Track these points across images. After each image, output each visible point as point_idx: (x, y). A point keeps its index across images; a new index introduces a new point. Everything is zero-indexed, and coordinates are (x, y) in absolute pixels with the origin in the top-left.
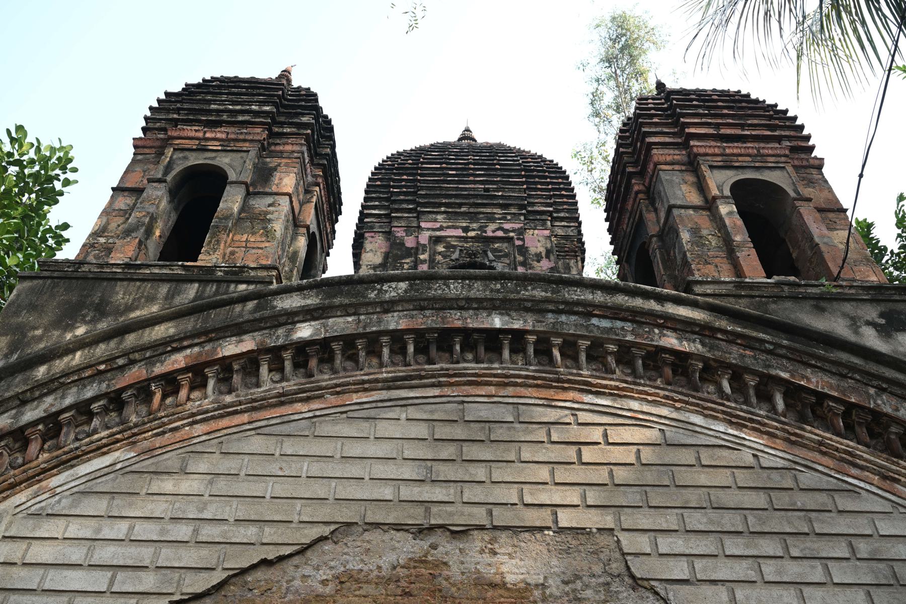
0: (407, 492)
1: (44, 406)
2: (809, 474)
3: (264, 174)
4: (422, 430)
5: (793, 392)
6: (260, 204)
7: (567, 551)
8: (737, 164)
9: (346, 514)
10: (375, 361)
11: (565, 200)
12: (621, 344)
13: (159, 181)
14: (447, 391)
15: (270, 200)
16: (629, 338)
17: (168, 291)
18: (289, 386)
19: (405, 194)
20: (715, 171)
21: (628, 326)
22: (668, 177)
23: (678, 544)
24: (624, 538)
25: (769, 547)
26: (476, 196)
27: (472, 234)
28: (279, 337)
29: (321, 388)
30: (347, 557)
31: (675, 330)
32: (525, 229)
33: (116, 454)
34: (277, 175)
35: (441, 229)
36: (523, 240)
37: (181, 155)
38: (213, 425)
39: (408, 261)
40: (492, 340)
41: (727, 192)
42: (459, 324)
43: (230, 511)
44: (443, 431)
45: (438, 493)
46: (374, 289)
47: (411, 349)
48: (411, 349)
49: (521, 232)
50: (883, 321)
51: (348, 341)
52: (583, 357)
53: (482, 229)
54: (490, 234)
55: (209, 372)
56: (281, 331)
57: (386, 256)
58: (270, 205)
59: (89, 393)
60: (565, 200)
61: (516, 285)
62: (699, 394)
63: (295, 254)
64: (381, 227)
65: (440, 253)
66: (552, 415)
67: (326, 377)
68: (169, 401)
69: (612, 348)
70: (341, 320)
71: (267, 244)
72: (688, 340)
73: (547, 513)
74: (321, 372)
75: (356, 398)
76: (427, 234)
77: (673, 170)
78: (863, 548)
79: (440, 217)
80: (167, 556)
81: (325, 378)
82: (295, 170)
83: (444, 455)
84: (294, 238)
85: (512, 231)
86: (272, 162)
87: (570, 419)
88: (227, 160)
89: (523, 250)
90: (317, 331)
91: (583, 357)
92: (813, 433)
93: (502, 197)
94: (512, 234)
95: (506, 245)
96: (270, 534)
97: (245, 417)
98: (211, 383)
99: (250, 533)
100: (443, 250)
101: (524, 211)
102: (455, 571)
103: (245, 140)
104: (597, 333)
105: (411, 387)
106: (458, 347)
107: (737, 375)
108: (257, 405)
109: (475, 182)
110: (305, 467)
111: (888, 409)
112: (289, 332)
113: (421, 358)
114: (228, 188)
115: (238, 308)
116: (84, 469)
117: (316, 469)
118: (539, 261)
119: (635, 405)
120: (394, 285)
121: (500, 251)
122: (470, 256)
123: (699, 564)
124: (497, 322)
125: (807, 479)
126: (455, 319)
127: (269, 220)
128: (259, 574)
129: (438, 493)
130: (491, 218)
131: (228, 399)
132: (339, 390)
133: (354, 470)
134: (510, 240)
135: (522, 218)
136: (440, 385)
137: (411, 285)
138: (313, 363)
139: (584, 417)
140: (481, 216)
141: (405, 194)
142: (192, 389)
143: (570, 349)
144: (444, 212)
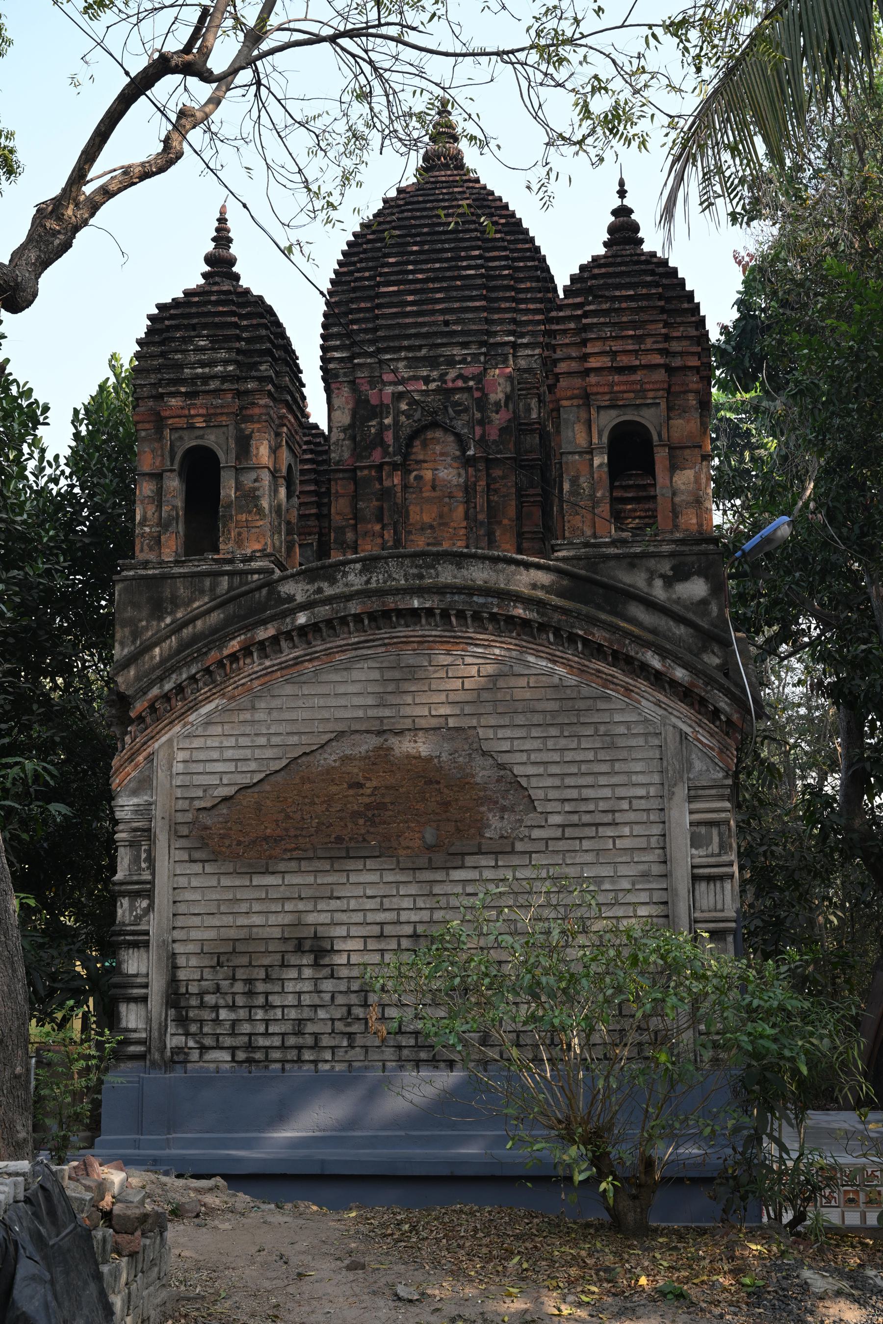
0: (371, 713)
1: (173, 680)
2: (587, 688)
3: (244, 445)
4: (376, 675)
5: (586, 642)
6: (248, 479)
7: (452, 739)
8: (621, 403)
9: (340, 727)
10: (346, 629)
11: (531, 317)
13: (171, 471)
15: (253, 475)
16: (495, 610)
18: (298, 653)
19: (366, 331)
20: (602, 412)
21: (495, 601)
22: (565, 416)
23: (508, 733)
24: (480, 731)
25: (554, 731)
26: (435, 334)
27: (433, 386)
29: (316, 652)
30: (345, 748)
31: (523, 603)
32: (485, 369)
33: (217, 701)
34: (253, 442)
37: (177, 435)
38: (263, 680)
39: (374, 423)
40: (415, 613)
41: (605, 439)
42: (392, 606)
43: (281, 729)
44: (388, 675)
45: (387, 712)
46: (340, 571)
47: (366, 622)
48: (366, 622)
49: (479, 378)
50: (671, 573)
51: (329, 622)
52: (469, 621)
53: (442, 378)
54: (450, 385)
56: (288, 620)
57: (354, 414)
58: (256, 481)
59: (194, 671)
60: (531, 317)
61: (433, 560)
62: (538, 641)
63: (279, 506)
64: (345, 375)
65: (403, 412)
66: (448, 660)
67: (319, 643)
68: (234, 666)
69: (485, 615)
70: (322, 609)
71: (261, 523)
72: (530, 610)
73: (442, 720)
74: (315, 639)
75: (338, 657)
76: (389, 390)
77: (572, 406)
78: (602, 729)
79: (401, 365)
80: (258, 753)
81: (319, 646)
82: (266, 435)
83: (389, 690)
84: (276, 491)
85: (472, 379)
86: (248, 427)
87: (459, 662)
88: (213, 438)
89: (482, 404)
90: (309, 619)
91: (469, 621)
93: (462, 333)
94: (471, 383)
95: (466, 395)
96: (304, 739)
97: (279, 674)
98: (255, 655)
99: (295, 739)
100: (406, 407)
101: (484, 350)
102: (397, 752)
103: (222, 414)
104: (476, 608)
105: (369, 647)
106: (394, 619)
107: (557, 632)
109: (433, 312)
111: (632, 653)
112: (294, 620)
113: (373, 625)
114: (222, 473)
116: (204, 710)
117: (322, 702)
118: (497, 413)
119: (497, 651)
120: (352, 566)
121: (460, 404)
122: (431, 414)
123: (516, 743)
124: (416, 604)
125: (585, 691)
126: (391, 602)
127: (258, 497)
128: (304, 759)
129: (387, 712)
130: (451, 362)
131: (268, 663)
132: (328, 653)
133: (342, 702)
134: (469, 389)
135: (482, 358)
136: (385, 645)
137: (363, 566)
138: (310, 636)
139: (469, 660)
140: (442, 359)
141: (366, 331)
142: (245, 656)
143: (461, 615)
144: (406, 358)
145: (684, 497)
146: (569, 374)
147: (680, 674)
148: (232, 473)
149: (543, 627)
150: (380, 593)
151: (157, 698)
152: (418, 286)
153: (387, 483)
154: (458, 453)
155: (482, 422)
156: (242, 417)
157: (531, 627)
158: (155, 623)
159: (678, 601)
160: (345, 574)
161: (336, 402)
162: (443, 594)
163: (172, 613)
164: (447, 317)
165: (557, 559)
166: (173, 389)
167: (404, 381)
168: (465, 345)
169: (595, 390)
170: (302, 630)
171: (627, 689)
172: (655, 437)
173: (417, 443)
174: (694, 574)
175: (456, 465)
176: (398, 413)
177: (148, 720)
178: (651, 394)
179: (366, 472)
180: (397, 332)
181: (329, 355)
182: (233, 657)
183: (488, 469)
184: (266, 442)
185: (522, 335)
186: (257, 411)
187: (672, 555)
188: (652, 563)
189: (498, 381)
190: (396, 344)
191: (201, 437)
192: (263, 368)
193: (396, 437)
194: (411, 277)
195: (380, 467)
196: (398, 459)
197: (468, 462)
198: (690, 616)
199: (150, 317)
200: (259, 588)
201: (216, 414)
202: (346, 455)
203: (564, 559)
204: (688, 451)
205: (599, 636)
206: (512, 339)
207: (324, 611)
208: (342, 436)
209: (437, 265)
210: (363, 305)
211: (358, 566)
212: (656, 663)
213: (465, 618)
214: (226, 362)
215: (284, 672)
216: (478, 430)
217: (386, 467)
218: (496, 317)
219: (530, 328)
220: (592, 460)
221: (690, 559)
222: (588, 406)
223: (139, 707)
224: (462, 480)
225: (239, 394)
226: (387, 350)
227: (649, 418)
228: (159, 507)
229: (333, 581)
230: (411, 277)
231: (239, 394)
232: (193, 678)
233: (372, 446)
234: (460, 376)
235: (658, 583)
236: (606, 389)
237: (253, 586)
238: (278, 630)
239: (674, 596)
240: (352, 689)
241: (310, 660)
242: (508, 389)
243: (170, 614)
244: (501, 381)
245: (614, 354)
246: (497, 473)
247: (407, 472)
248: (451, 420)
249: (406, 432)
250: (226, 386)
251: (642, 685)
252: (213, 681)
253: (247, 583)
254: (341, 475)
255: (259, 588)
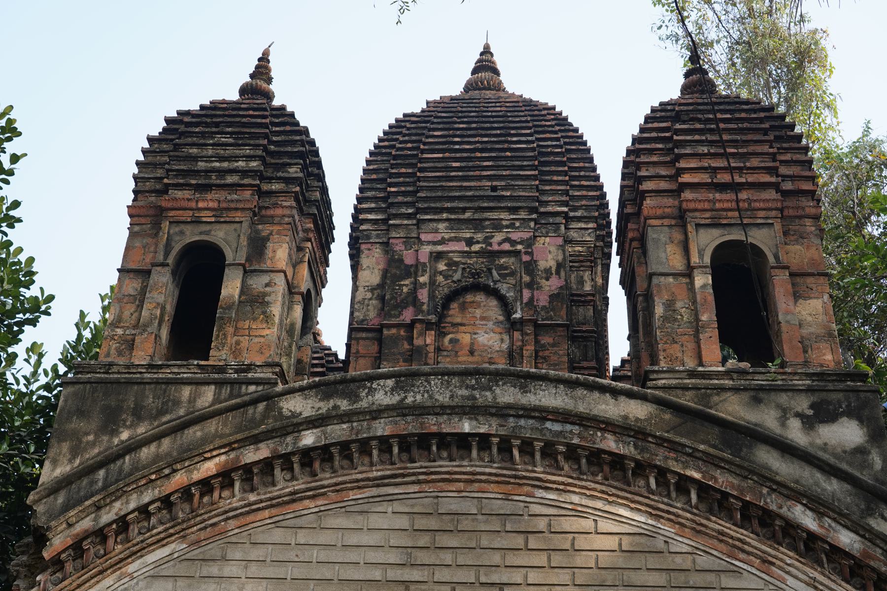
0: (392, 574)
1: (115, 510)
2: (706, 558)
3: (258, 246)
4: (403, 522)
5: (703, 489)
6: (257, 283)
8: (725, 222)
10: (366, 460)
11: (584, 193)
12: (569, 446)
13: (163, 265)
14: (425, 487)
15: (265, 279)
16: (576, 441)
17: (190, 394)
18: (298, 485)
19: (404, 194)
20: (702, 231)
21: (576, 429)
22: (655, 236)
26: (481, 198)
27: (476, 248)
28: (287, 445)
29: (323, 487)
31: (614, 433)
32: (535, 237)
33: (173, 546)
34: (270, 245)
35: (442, 242)
36: (531, 254)
37: (177, 229)
39: (407, 282)
40: (463, 442)
41: (707, 260)
42: (434, 429)
44: (422, 523)
45: (415, 575)
46: (365, 387)
47: (396, 450)
48: (396, 450)
49: (529, 243)
50: (810, 412)
51: (344, 446)
52: (538, 456)
53: (487, 240)
54: (496, 247)
55: (236, 476)
56: (289, 439)
57: (385, 274)
58: (267, 285)
59: (146, 498)
60: (584, 193)
61: (489, 380)
62: (632, 489)
63: (292, 325)
64: (378, 236)
65: (441, 273)
67: (328, 475)
68: (206, 499)
69: (562, 448)
70: (337, 427)
71: (267, 332)
72: (624, 442)
74: (323, 470)
75: (352, 495)
76: (427, 249)
77: (662, 225)
79: (441, 226)
81: (327, 478)
82: (287, 239)
84: (290, 308)
85: (520, 243)
86: (265, 229)
89: (530, 267)
91: (538, 456)
92: (716, 524)
93: (511, 198)
94: (519, 247)
95: (512, 260)
97: (266, 513)
98: (237, 485)
100: (445, 268)
101: (534, 216)
103: (236, 209)
104: (549, 437)
105: (396, 485)
106: (434, 448)
108: (275, 503)
109: (480, 178)
110: (316, 554)
111: (773, 507)
112: (297, 439)
113: (405, 456)
114: (227, 271)
115: (251, 410)
116: (151, 558)
117: (323, 556)
118: (547, 279)
119: (576, 499)
120: (382, 382)
121: (506, 268)
122: (473, 275)
124: (466, 427)
125: (703, 561)
126: (432, 424)
127: (268, 303)
129: (415, 575)
130: (497, 226)
131: (252, 497)
132: (338, 488)
133: (352, 556)
134: (517, 253)
135: (532, 224)
136: (419, 482)
137: (397, 382)
138: (317, 465)
140: (487, 223)
141: (404, 194)
142: (222, 488)
143: (527, 448)
145: (812, 330)
146: (658, 192)
147: (846, 539)
148: (240, 273)
149: (641, 469)
150: (420, 411)
151: (87, 535)
152: (465, 155)
153: (418, 342)
154: (501, 318)
155: (530, 286)
156: (258, 215)
157: (623, 469)
158: (105, 438)
159: (825, 447)
160: (371, 391)
161: (365, 261)
162: (505, 416)
163: (132, 426)
164: (495, 183)
165: (656, 388)
166: (181, 181)
167: (440, 243)
168: (514, 210)
169: (692, 206)
170: (307, 456)
171: (764, 561)
172: (771, 259)
173: (454, 305)
174: (843, 414)
175: (499, 330)
176: (435, 273)
177: (69, 567)
178: (762, 214)
179: (394, 331)
180: (439, 194)
181: (361, 217)
182: (206, 485)
183: (536, 335)
184: (285, 246)
185: (575, 209)
186: (279, 212)
187: (809, 390)
188: (783, 398)
189: (548, 252)
190: (438, 205)
191: (207, 233)
192: (292, 170)
193: (432, 297)
194: (457, 147)
195: (410, 326)
196: (433, 318)
197: (512, 326)
198: (844, 466)
199: (168, 120)
200: (255, 402)
201: (228, 209)
202: (372, 314)
203: (664, 388)
204: (810, 280)
205: (723, 480)
206: (565, 209)
207: (339, 431)
208: (369, 295)
209: (486, 139)
210: (403, 170)
211: (390, 383)
212: (808, 521)
213: (532, 455)
214: (250, 158)
215: (274, 511)
216: (526, 294)
217: (418, 325)
218: (547, 188)
219: (584, 202)
220: (692, 283)
221: (834, 396)
222: (684, 226)
223: (58, 542)
224: (505, 346)
225: (261, 194)
226: (426, 211)
227: (760, 238)
228: (140, 307)
229: (354, 397)
230: (457, 147)
231: (261, 194)
232: (143, 511)
233: (402, 306)
234: (507, 240)
235: (795, 424)
236: (707, 206)
237: (247, 398)
238: (274, 451)
239: (819, 441)
240: (366, 539)
241: (313, 497)
242: (560, 258)
243: (130, 427)
244: (553, 249)
245: (714, 170)
246: (546, 340)
247: (441, 334)
248: (495, 282)
249: (444, 286)
250: (246, 181)
251: (786, 555)
252: (173, 519)
253: (239, 395)
254: (364, 335)
255: (255, 402)
